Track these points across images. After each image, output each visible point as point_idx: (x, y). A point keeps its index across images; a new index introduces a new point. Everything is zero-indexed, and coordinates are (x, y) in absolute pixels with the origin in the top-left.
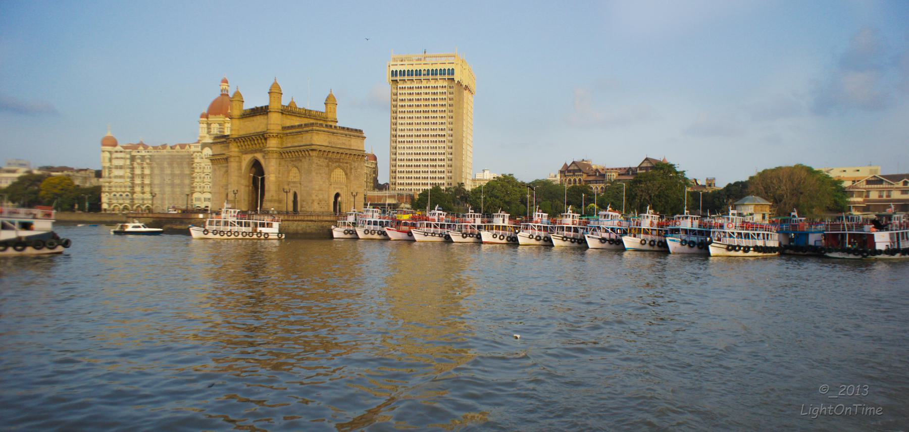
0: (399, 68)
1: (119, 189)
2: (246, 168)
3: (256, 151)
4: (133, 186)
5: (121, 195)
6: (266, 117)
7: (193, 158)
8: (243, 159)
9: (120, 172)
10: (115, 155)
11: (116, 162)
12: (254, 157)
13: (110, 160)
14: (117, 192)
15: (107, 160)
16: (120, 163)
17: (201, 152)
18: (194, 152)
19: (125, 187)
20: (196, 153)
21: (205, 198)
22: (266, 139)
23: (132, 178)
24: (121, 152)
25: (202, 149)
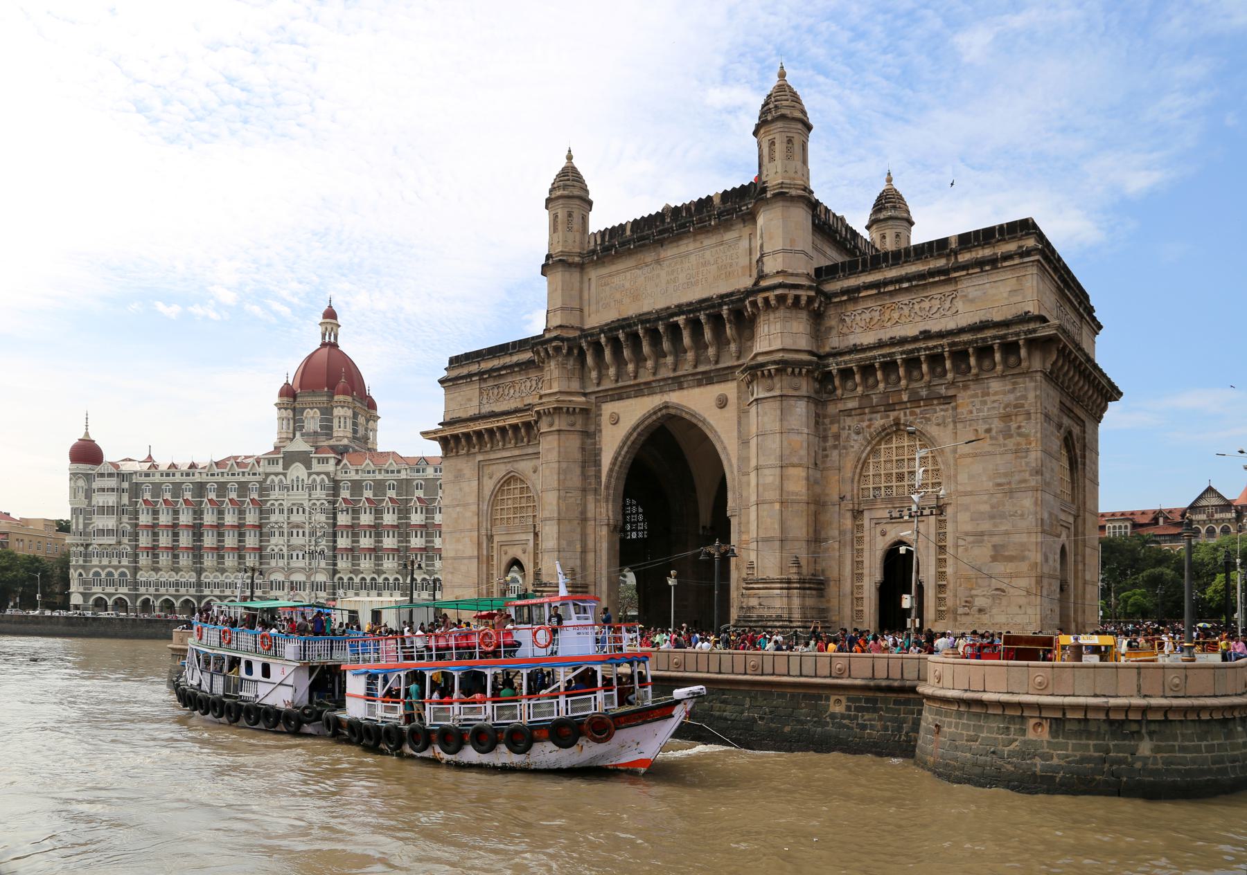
1: (105, 562)
2: (618, 454)
3: (678, 383)
5: (110, 574)
6: (746, 231)
7: (266, 489)
8: (605, 419)
9: (109, 522)
11: (99, 500)
12: (666, 406)
13: (89, 494)
15: (81, 495)
16: (111, 499)
18: (267, 475)
19: (120, 555)
20: (273, 477)
24: (110, 475)
25: (286, 467)
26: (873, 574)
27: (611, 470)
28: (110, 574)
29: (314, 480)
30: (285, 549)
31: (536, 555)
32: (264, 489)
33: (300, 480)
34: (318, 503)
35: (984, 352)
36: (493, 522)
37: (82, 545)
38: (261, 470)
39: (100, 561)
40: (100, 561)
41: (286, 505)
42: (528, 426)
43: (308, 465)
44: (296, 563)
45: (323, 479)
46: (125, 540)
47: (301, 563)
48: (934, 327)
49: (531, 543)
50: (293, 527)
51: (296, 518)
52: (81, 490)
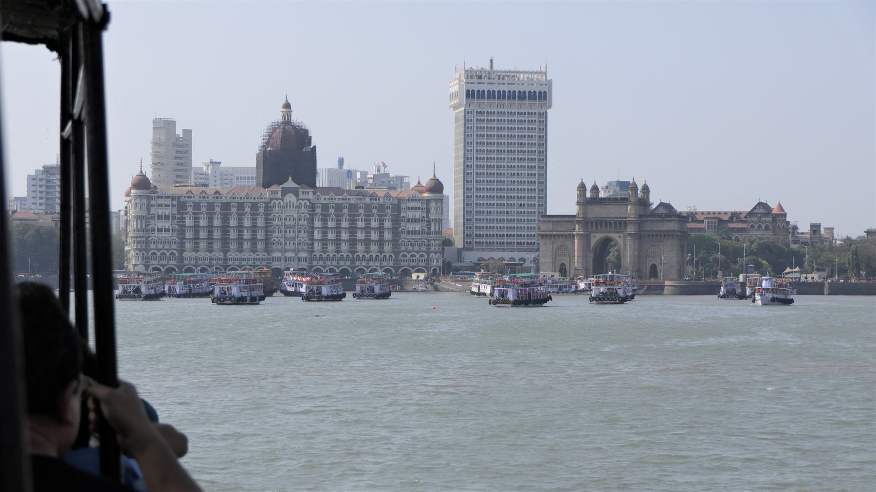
0: (476, 87)
1: (160, 246)
2: (594, 244)
3: (610, 232)
4: (182, 242)
7: (271, 207)
8: (592, 237)
9: (167, 225)
10: (159, 202)
12: (607, 236)
13: (148, 209)
14: (159, 251)
16: (167, 211)
17: (283, 200)
18: (271, 199)
20: (275, 201)
21: (286, 258)
22: (627, 224)
23: (182, 230)
26: (648, 269)
27: (593, 247)
28: (163, 254)
29: (300, 203)
30: (282, 240)
31: (570, 263)
32: (268, 207)
33: (292, 202)
34: (303, 215)
35: (669, 235)
36: (556, 255)
37: (140, 237)
38: (268, 196)
39: (156, 247)
40: (156, 247)
41: (283, 216)
42: (570, 235)
43: (297, 195)
44: (288, 247)
45: (305, 203)
46: (175, 234)
47: (292, 247)
48: (661, 229)
49: (568, 260)
50: (287, 228)
51: (288, 223)
52: (143, 205)
